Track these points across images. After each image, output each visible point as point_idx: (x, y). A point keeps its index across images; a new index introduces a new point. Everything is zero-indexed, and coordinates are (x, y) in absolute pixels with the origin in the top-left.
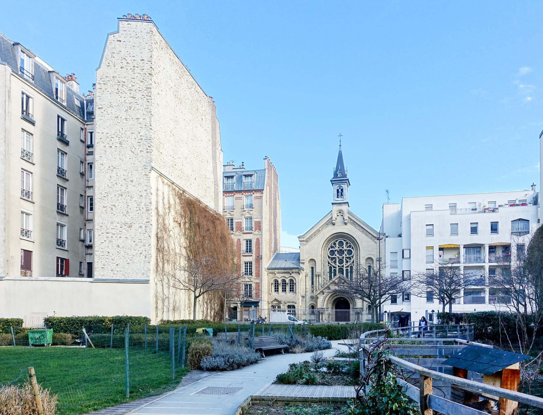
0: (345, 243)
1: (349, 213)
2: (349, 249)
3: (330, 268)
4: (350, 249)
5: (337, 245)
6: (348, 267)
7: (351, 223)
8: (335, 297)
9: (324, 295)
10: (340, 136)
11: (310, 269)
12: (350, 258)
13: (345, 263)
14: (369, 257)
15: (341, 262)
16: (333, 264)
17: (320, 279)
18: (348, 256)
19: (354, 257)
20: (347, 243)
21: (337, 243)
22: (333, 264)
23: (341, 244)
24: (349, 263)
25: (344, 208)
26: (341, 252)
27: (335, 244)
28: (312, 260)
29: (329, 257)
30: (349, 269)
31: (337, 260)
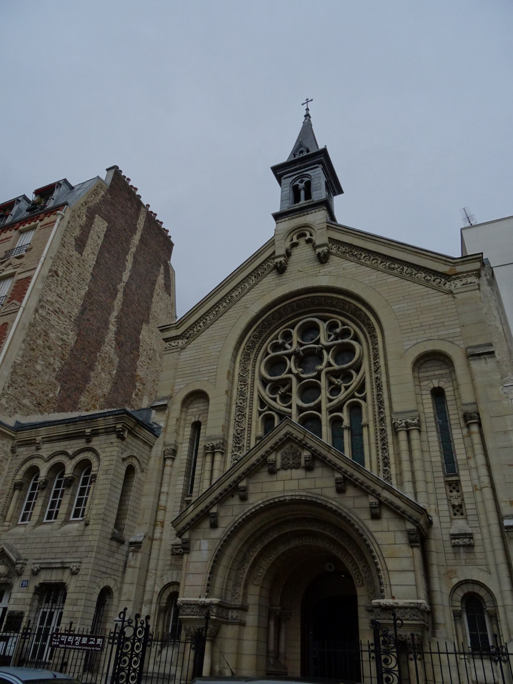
0: (323, 326)
6: (339, 408)
7: (343, 256)
8: (282, 549)
10: (308, 101)
11: (188, 431)
12: (346, 375)
14: (430, 347)
16: (279, 405)
18: (336, 367)
20: (332, 326)
21: (294, 333)
22: (279, 405)
24: (342, 396)
29: (264, 382)
31: (295, 386)
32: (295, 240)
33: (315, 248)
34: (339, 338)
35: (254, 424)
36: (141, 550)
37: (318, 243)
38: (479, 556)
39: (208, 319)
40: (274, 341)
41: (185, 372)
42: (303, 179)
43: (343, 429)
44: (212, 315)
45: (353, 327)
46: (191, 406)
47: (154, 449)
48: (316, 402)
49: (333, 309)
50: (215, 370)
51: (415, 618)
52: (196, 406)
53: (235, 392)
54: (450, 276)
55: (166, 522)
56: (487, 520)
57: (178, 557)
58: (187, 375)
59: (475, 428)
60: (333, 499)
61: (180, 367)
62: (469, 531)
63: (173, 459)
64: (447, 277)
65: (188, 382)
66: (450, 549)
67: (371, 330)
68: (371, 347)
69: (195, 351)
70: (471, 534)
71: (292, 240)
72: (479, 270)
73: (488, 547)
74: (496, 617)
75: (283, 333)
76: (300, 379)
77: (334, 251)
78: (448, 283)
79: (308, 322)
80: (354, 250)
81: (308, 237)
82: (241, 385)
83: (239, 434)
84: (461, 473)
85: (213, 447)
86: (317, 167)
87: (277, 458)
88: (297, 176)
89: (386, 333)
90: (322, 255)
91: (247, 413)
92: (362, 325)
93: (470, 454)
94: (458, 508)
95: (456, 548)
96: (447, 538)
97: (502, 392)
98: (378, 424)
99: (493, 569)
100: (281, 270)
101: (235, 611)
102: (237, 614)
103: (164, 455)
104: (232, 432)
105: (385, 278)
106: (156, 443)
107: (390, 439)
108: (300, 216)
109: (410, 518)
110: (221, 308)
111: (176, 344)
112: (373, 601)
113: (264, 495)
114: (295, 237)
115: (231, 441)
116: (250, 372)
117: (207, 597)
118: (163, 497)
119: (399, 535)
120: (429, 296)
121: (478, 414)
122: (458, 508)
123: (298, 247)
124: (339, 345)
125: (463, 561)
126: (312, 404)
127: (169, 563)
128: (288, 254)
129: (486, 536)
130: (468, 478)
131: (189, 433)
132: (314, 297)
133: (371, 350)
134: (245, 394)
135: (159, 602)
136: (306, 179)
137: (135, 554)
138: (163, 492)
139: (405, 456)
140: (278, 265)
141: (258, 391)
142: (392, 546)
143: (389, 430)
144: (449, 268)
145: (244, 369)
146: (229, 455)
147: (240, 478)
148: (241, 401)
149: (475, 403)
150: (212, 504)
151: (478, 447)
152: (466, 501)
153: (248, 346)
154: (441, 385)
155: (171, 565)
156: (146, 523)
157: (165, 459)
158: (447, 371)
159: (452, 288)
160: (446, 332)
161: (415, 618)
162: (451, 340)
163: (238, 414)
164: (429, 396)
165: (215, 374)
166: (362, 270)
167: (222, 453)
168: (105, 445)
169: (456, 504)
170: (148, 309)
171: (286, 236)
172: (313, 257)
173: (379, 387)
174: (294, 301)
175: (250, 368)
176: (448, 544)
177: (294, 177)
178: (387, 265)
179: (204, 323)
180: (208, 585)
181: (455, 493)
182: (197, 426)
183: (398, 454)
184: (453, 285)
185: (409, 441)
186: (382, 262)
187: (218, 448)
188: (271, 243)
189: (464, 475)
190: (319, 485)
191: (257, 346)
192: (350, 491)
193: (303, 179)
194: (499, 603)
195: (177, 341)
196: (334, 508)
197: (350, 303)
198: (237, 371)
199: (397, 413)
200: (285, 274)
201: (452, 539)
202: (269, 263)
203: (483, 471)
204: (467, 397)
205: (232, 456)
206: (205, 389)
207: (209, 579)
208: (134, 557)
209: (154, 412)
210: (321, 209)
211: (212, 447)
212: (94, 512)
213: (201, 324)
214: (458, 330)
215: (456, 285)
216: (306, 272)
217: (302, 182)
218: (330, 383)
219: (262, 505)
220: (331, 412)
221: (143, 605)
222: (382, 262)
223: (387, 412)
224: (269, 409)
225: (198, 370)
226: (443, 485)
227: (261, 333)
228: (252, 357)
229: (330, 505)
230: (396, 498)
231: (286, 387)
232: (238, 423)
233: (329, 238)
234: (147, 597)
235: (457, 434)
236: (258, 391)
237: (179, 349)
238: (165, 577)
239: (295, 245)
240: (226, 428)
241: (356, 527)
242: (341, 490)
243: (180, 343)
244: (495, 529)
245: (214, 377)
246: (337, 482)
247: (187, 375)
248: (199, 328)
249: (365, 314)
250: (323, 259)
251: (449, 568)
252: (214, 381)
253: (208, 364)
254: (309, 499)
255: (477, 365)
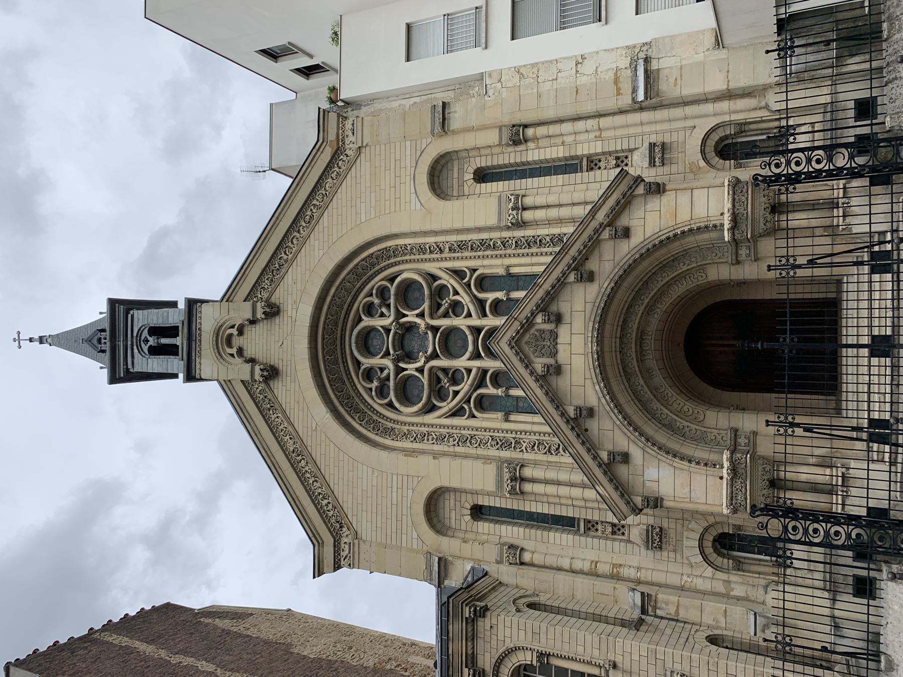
0: (367, 322)
1: (229, 296)
2: (392, 301)
3: (483, 404)
4: (392, 291)
5: (376, 361)
6: (481, 303)
7: (275, 284)
8: (659, 379)
9: (636, 453)
11: (484, 527)
13: (460, 322)
15: (450, 342)
16: (464, 387)
17: (538, 473)
18: (426, 306)
19: (432, 268)
20: (369, 310)
21: (367, 362)
22: (464, 387)
23: (366, 341)
24: (464, 298)
25: (208, 320)
26: (405, 341)
27: (369, 375)
28: (434, 504)
29: (430, 408)
30: (490, 296)
31: (443, 362)
32: (234, 351)
33: (253, 322)
34: (388, 302)
35: (485, 424)
36: (654, 594)
37: (249, 316)
38: (674, 138)
39: (320, 491)
40: (374, 393)
41: (394, 530)
42: (143, 338)
43: (509, 299)
44: (315, 484)
45: (377, 281)
46: (447, 521)
47: (505, 579)
48: (468, 332)
49: (346, 307)
50: (400, 477)
51: (744, 190)
52: (447, 516)
53: (436, 447)
54: (338, 148)
55: (614, 562)
56: (636, 125)
57: (664, 540)
58: (399, 527)
59: (530, 132)
60: (600, 288)
61: (384, 541)
62: (646, 145)
63: (522, 549)
64: (338, 152)
65: (410, 523)
66: (666, 169)
67: (386, 254)
68: (408, 257)
69: (364, 513)
70: (650, 144)
71: (232, 355)
72: (339, 115)
73: (665, 126)
74: (741, 124)
75: (364, 380)
76: (434, 356)
77: (265, 295)
78: (348, 152)
79: (356, 343)
80: (272, 268)
81: (234, 331)
82: (428, 440)
83: (497, 443)
84: (579, 153)
85: (513, 479)
86: (132, 316)
87: (539, 363)
88: (135, 347)
89: (395, 230)
90: (268, 310)
91: (469, 432)
92: (377, 268)
93: (559, 140)
94: (619, 162)
95: (665, 161)
96: (653, 171)
97: (493, 97)
98: (509, 251)
99: (690, 123)
100: (272, 373)
101: (739, 440)
102: (743, 437)
103: (516, 564)
104: (493, 452)
105: (321, 230)
106: (496, 576)
107: (529, 232)
108: (200, 341)
109: (631, 188)
110: (307, 468)
111: (347, 547)
112: (726, 239)
113: (588, 382)
114: (229, 351)
115: (506, 454)
116: (411, 428)
117: (722, 467)
118: (578, 565)
119: (649, 206)
120: (358, 175)
121: (514, 126)
122: (619, 162)
123: (245, 348)
124: (396, 300)
125: (680, 155)
126: (470, 338)
127: (672, 555)
128: (252, 361)
129: (653, 128)
130: (586, 145)
131: (486, 524)
132: (324, 328)
133: (413, 257)
134: (441, 435)
135: (727, 571)
136: (146, 332)
137: (659, 605)
138: (571, 565)
139: (553, 213)
140: (265, 373)
141: (440, 417)
142: (662, 216)
143: (518, 234)
144: (327, 147)
145: (405, 435)
146: (526, 456)
147: (563, 414)
148: (451, 439)
149: (500, 128)
150: (595, 457)
151: (553, 129)
152: (612, 149)
153: (373, 429)
154: (472, 171)
155: (675, 551)
156: (615, 588)
157: (522, 564)
158: (456, 163)
159: (355, 146)
160: (408, 158)
161: (744, 190)
162: (419, 153)
163: (468, 444)
164: (483, 185)
165: (405, 478)
166: (303, 258)
167: (522, 466)
168: (494, 642)
169: (614, 162)
170: (267, 643)
171: (224, 363)
172: (265, 326)
173: (462, 246)
174: (324, 357)
175: (405, 428)
176: (660, 170)
177: (136, 351)
178: (304, 225)
179: (324, 498)
180: (706, 465)
181: (602, 164)
182: (478, 512)
183: (549, 222)
184: (351, 146)
185: (535, 208)
186: (299, 232)
187: (515, 470)
188: (227, 387)
189: (582, 150)
190: (581, 305)
191: (375, 417)
192: (592, 265)
193: (143, 338)
194: (727, 118)
195: (343, 545)
196: (612, 285)
197: (344, 279)
198: (407, 444)
199: (500, 220)
200: (281, 368)
201: (654, 166)
202: (257, 396)
203: (581, 125)
204: (492, 137)
205: (527, 452)
206: (426, 494)
207: (698, 463)
208: (664, 605)
209: (446, 582)
210: (199, 310)
211: (512, 481)
212: (596, 653)
213: (325, 502)
214: (408, 143)
215: (351, 143)
216: (285, 335)
217: (147, 341)
218: (446, 315)
219: (602, 385)
220: (485, 315)
221: (732, 593)
222: (299, 232)
223: (495, 235)
224: (469, 401)
225: (394, 507)
226: (592, 173)
227: (358, 410)
228: (390, 425)
229: (609, 290)
230: (607, 202)
231: (441, 376)
232: (482, 443)
233: (245, 301)
234: (720, 588)
235: (533, 154)
236: (440, 417)
237: (356, 541)
238: (693, 560)
239: (240, 351)
240: (487, 459)
241: (637, 256)
242: (590, 277)
243: (346, 540)
244: (646, 116)
245: (410, 479)
246: (580, 279)
247: (399, 527)
248: (330, 507)
249: (363, 260)
250: (273, 311)
251: (688, 170)
252: (415, 479)
253: (389, 490)
254: (598, 319)
255: (457, 120)
